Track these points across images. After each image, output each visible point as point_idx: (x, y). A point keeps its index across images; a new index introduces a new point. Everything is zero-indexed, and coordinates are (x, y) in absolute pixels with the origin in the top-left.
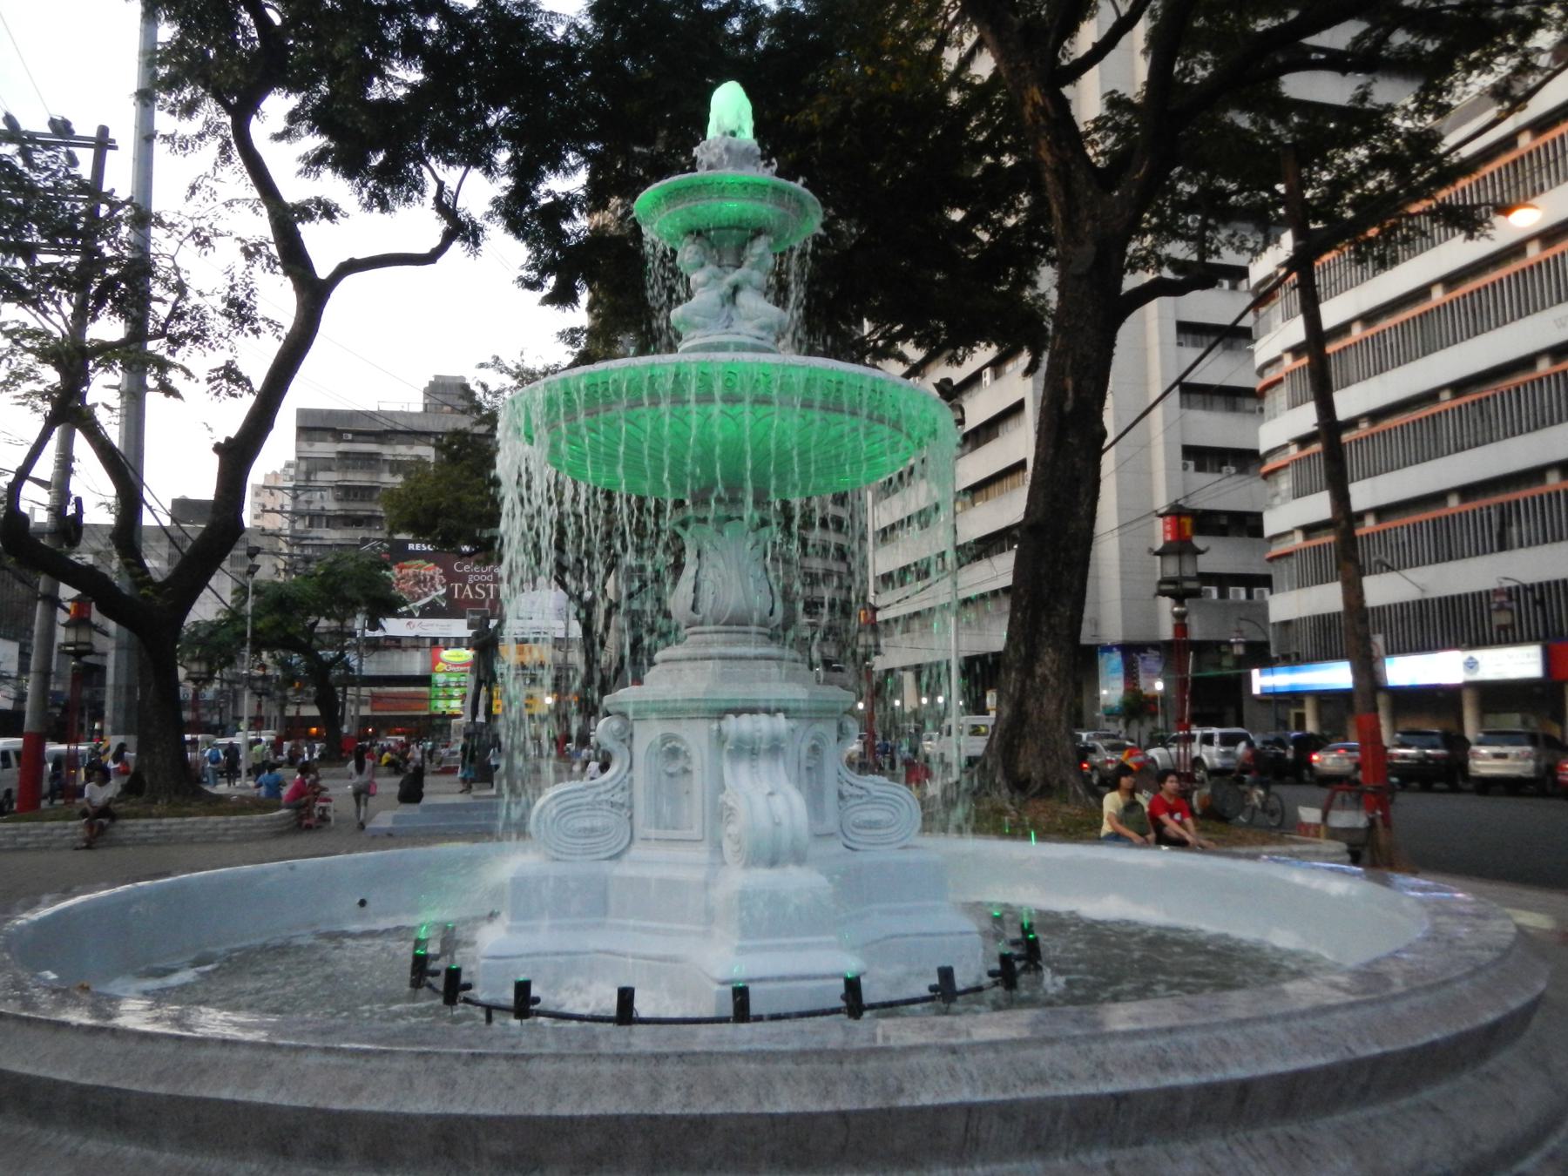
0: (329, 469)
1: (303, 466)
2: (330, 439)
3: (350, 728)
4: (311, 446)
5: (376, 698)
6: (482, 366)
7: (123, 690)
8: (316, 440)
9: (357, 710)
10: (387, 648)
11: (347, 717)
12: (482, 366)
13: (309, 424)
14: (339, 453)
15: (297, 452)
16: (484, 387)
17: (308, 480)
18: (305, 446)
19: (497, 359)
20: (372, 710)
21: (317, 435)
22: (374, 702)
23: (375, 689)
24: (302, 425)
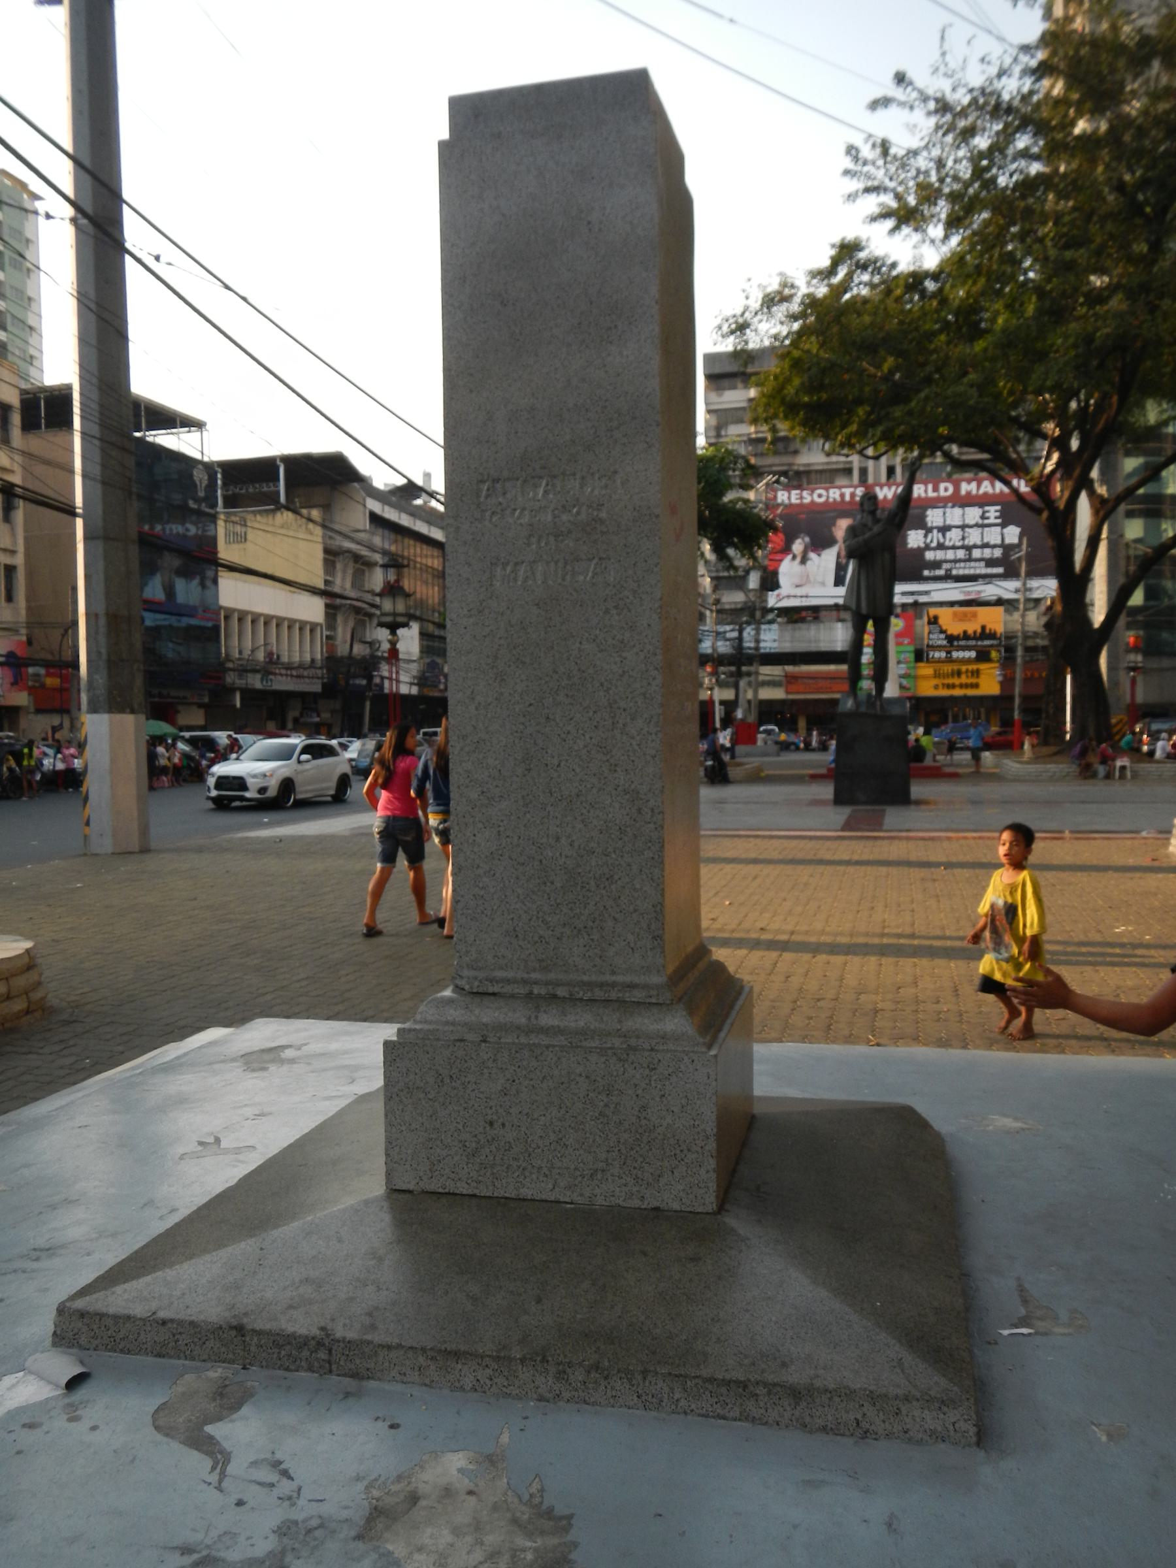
0: (740, 421)
1: (714, 422)
2: (740, 385)
3: (745, 712)
4: (720, 395)
5: (791, 679)
6: (875, 105)
7: (102, 621)
8: (724, 389)
9: (756, 693)
10: (803, 620)
11: (741, 701)
12: (875, 105)
13: (718, 370)
14: (751, 400)
15: (707, 404)
16: (885, 147)
17: (718, 436)
18: (714, 397)
19: (900, 79)
20: (788, 692)
21: (726, 382)
22: (789, 683)
23: (790, 668)
24: (707, 373)
